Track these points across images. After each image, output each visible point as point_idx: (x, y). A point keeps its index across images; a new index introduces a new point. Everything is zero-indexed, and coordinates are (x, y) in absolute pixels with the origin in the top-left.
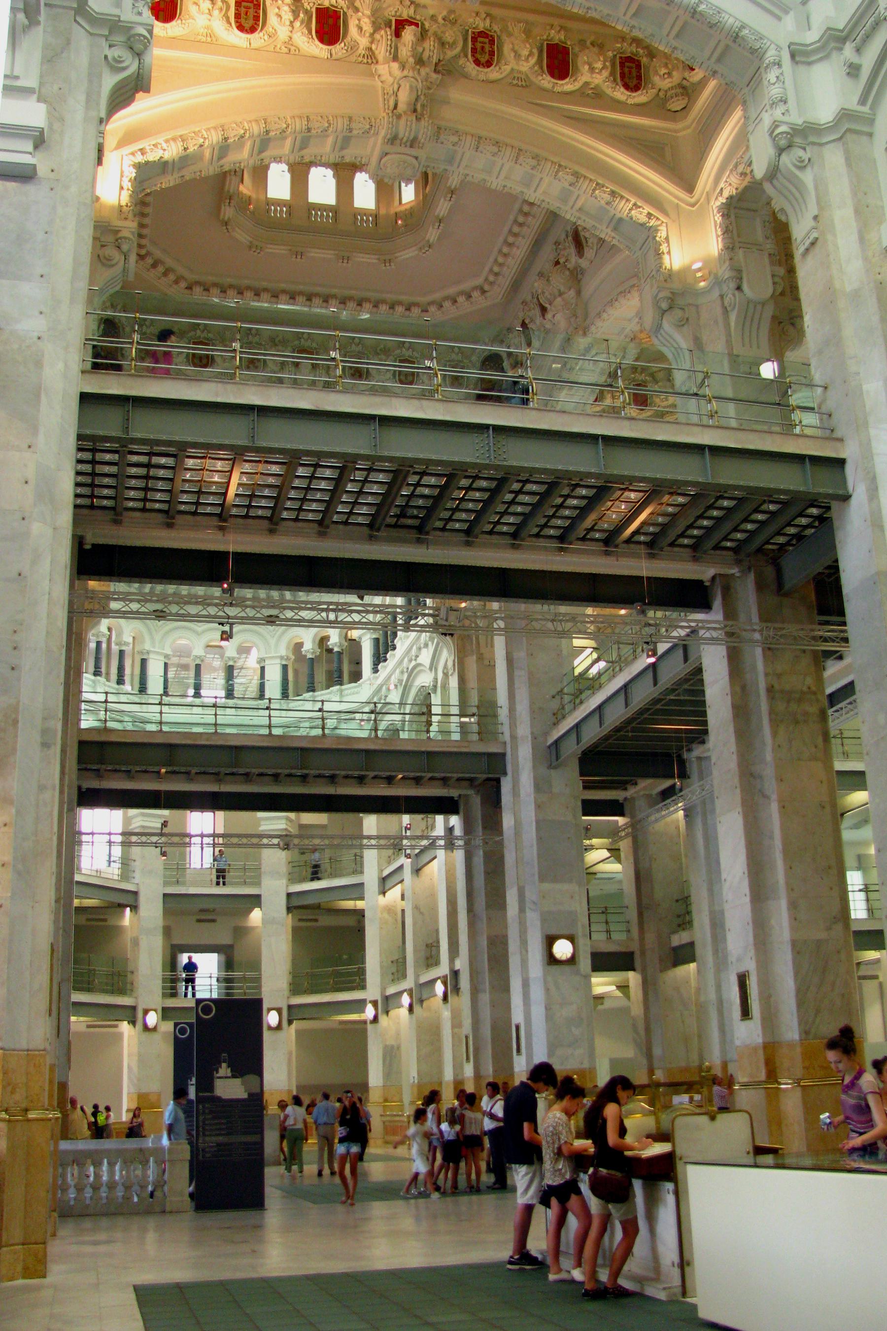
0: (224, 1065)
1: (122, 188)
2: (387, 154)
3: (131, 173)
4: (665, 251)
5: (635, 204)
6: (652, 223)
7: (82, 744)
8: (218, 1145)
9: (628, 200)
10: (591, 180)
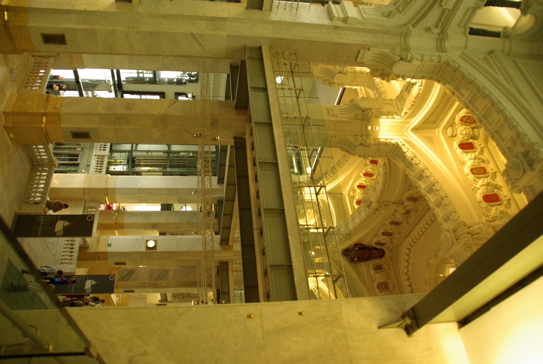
0: (68, 224)
1: (386, 139)
2: (448, 232)
3: (393, 142)
7: (227, 263)
8: (40, 222)
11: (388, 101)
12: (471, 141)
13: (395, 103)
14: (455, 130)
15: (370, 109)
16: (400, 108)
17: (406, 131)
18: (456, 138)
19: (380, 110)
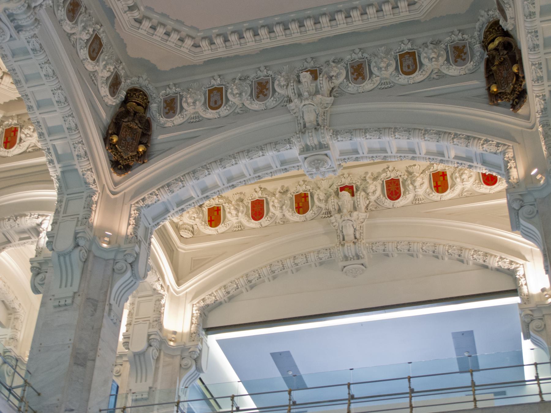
1: (192, 323)
2: (344, 267)
3: (196, 313)
4: (524, 283)
5: (501, 258)
6: (513, 267)
9: (495, 256)
10: (470, 250)
11: (133, 308)
12: (205, 209)
13: (137, 299)
14: (185, 226)
15: (149, 335)
16: (150, 293)
17: (177, 293)
18: (195, 227)
19: (151, 321)
